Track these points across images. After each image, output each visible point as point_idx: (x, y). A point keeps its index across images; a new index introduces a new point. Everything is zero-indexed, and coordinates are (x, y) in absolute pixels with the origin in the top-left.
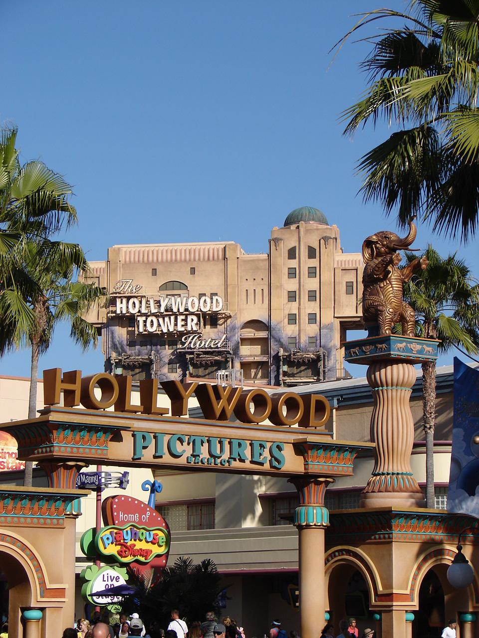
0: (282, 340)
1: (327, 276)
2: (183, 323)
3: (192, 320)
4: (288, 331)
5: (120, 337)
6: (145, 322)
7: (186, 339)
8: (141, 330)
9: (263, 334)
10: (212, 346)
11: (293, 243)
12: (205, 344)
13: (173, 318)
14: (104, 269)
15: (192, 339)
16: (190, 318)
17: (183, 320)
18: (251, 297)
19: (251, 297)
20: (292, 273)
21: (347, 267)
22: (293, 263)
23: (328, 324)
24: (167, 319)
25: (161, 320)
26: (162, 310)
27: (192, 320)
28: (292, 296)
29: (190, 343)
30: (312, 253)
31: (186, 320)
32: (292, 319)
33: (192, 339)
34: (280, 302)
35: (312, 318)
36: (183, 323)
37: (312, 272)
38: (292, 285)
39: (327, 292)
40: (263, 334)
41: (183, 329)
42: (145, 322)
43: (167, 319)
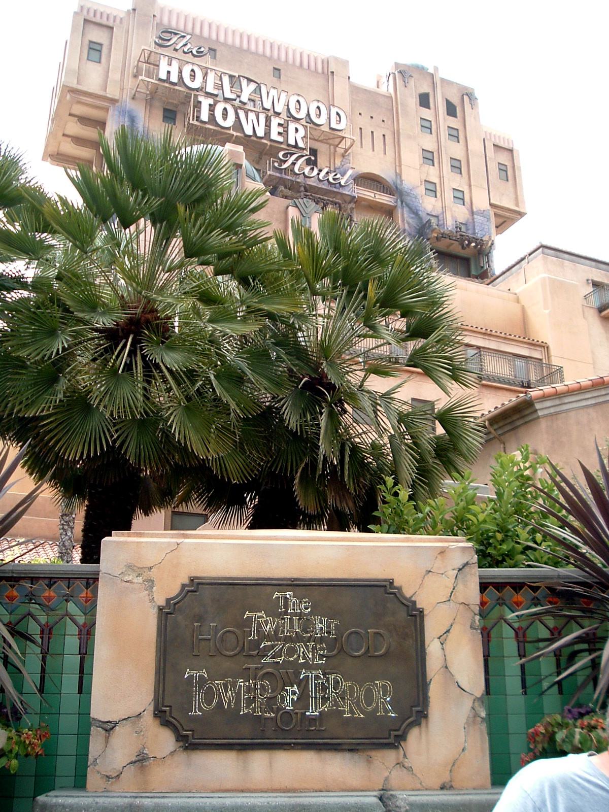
0: (420, 213)
1: (475, 146)
2: (281, 130)
3: (297, 130)
4: (429, 205)
5: (146, 132)
6: (212, 108)
7: (285, 155)
8: (205, 116)
9: (384, 199)
10: (331, 180)
11: (425, 88)
12: (318, 174)
13: (262, 117)
14: (121, 19)
15: (297, 159)
16: (292, 126)
17: (280, 125)
18: (367, 140)
19: (367, 140)
20: (426, 126)
21: (502, 144)
22: (427, 114)
23: (484, 211)
24: (252, 116)
25: (242, 114)
26: (244, 98)
27: (297, 130)
28: (429, 157)
29: (294, 164)
30: (451, 110)
31: (284, 126)
32: (432, 189)
33: (297, 159)
34: (411, 157)
35: (459, 197)
36: (281, 130)
37: (454, 135)
38: (429, 143)
39: (477, 164)
40: (384, 199)
41: (281, 139)
42: (212, 108)
43: (252, 116)
